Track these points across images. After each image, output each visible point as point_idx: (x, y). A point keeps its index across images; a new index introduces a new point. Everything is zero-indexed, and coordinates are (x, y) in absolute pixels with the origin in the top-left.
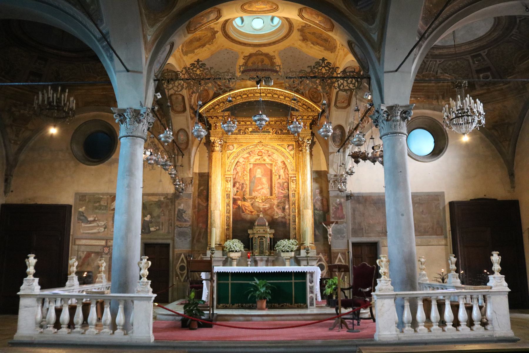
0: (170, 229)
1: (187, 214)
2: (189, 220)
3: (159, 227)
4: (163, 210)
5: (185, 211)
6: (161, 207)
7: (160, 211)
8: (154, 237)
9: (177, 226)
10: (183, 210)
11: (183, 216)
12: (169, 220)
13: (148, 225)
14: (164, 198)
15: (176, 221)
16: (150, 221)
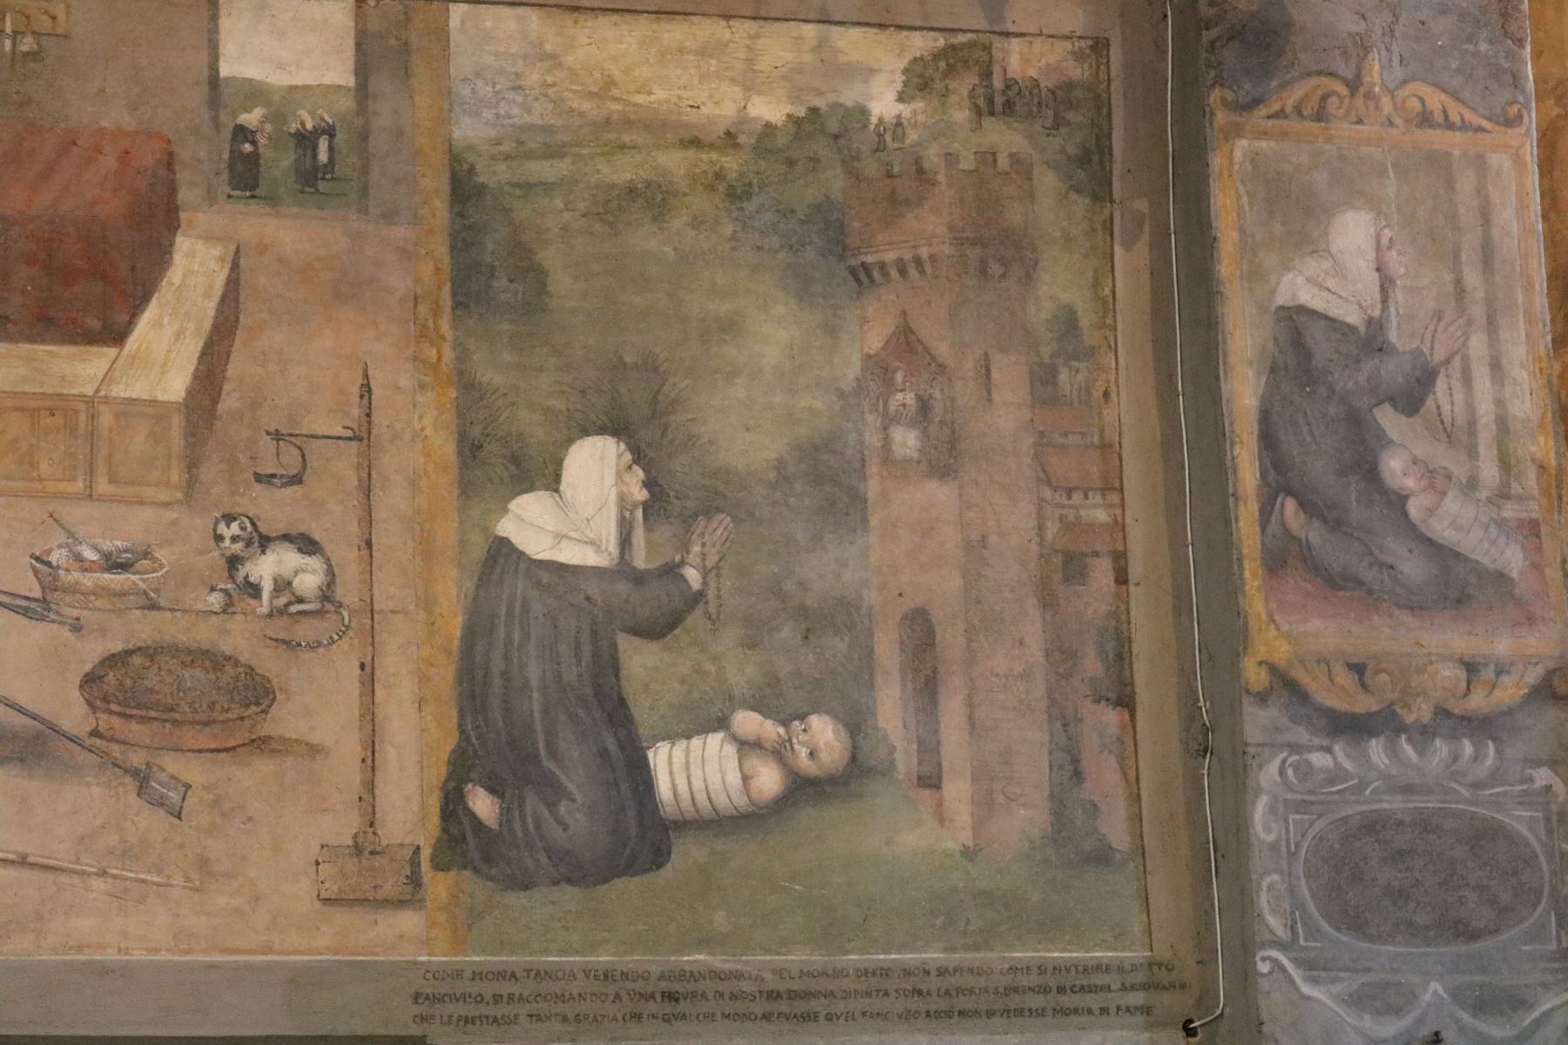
0: (1105, 777)
1: (1459, 436)
2: (1513, 559)
3: (855, 724)
4: (906, 341)
5: (1425, 380)
6: (863, 278)
7: (850, 369)
8: (758, 961)
9: (1286, 686)
10: (1372, 340)
11: (1394, 467)
12: (1074, 567)
13: (607, 667)
14: (918, 82)
15: (1252, 575)
16: (624, 570)
